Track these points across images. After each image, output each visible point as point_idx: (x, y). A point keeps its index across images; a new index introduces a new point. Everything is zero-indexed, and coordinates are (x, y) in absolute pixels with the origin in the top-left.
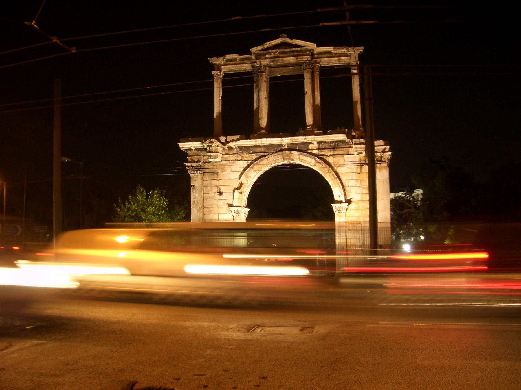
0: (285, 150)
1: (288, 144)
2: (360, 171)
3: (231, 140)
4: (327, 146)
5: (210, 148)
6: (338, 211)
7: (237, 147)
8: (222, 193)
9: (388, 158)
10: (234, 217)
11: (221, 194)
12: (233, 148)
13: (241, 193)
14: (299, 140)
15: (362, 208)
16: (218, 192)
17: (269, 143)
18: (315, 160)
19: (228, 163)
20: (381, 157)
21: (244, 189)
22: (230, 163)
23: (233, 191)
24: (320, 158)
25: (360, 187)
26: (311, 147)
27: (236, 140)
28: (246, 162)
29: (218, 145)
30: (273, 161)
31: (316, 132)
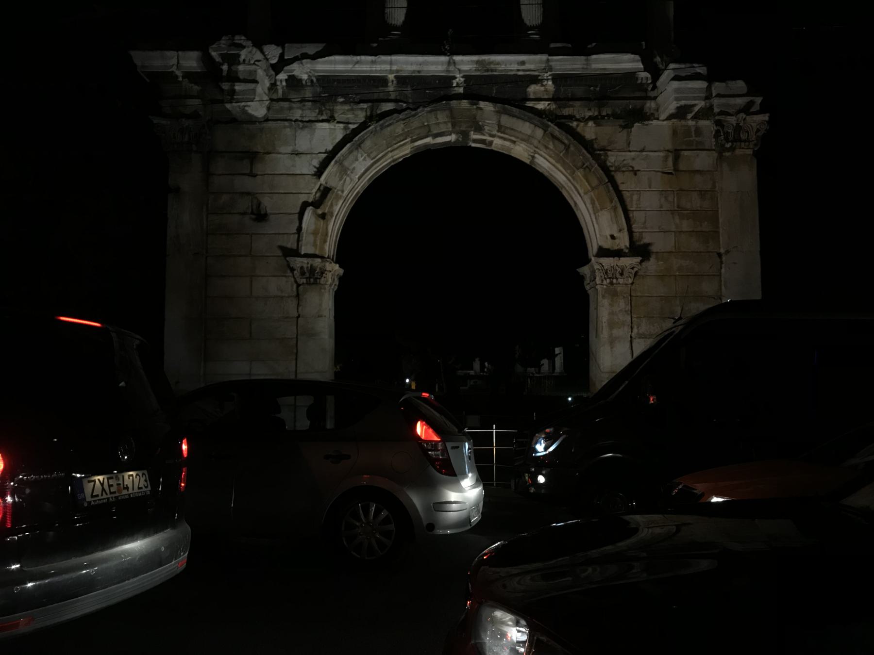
0: (459, 97)
1: (468, 78)
2: (672, 168)
3: (298, 54)
4: (579, 91)
5: (230, 66)
6: (608, 280)
7: (315, 80)
8: (266, 215)
9: (758, 130)
10: (301, 288)
11: (261, 217)
12: (304, 82)
13: (323, 216)
14: (503, 67)
15: (677, 273)
16: (252, 213)
17: (414, 71)
18: (545, 131)
19: (285, 127)
20: (738, 128)
21: (332, 205)
22: (290, 127)
23: (298, 210)
24: (559, 125)
25: (672, 214)
26: (534, 93)
27: (314, 57)
28: (342, 125)
29: (259, 61)
30: (420, 127)
31: (552, 45)
